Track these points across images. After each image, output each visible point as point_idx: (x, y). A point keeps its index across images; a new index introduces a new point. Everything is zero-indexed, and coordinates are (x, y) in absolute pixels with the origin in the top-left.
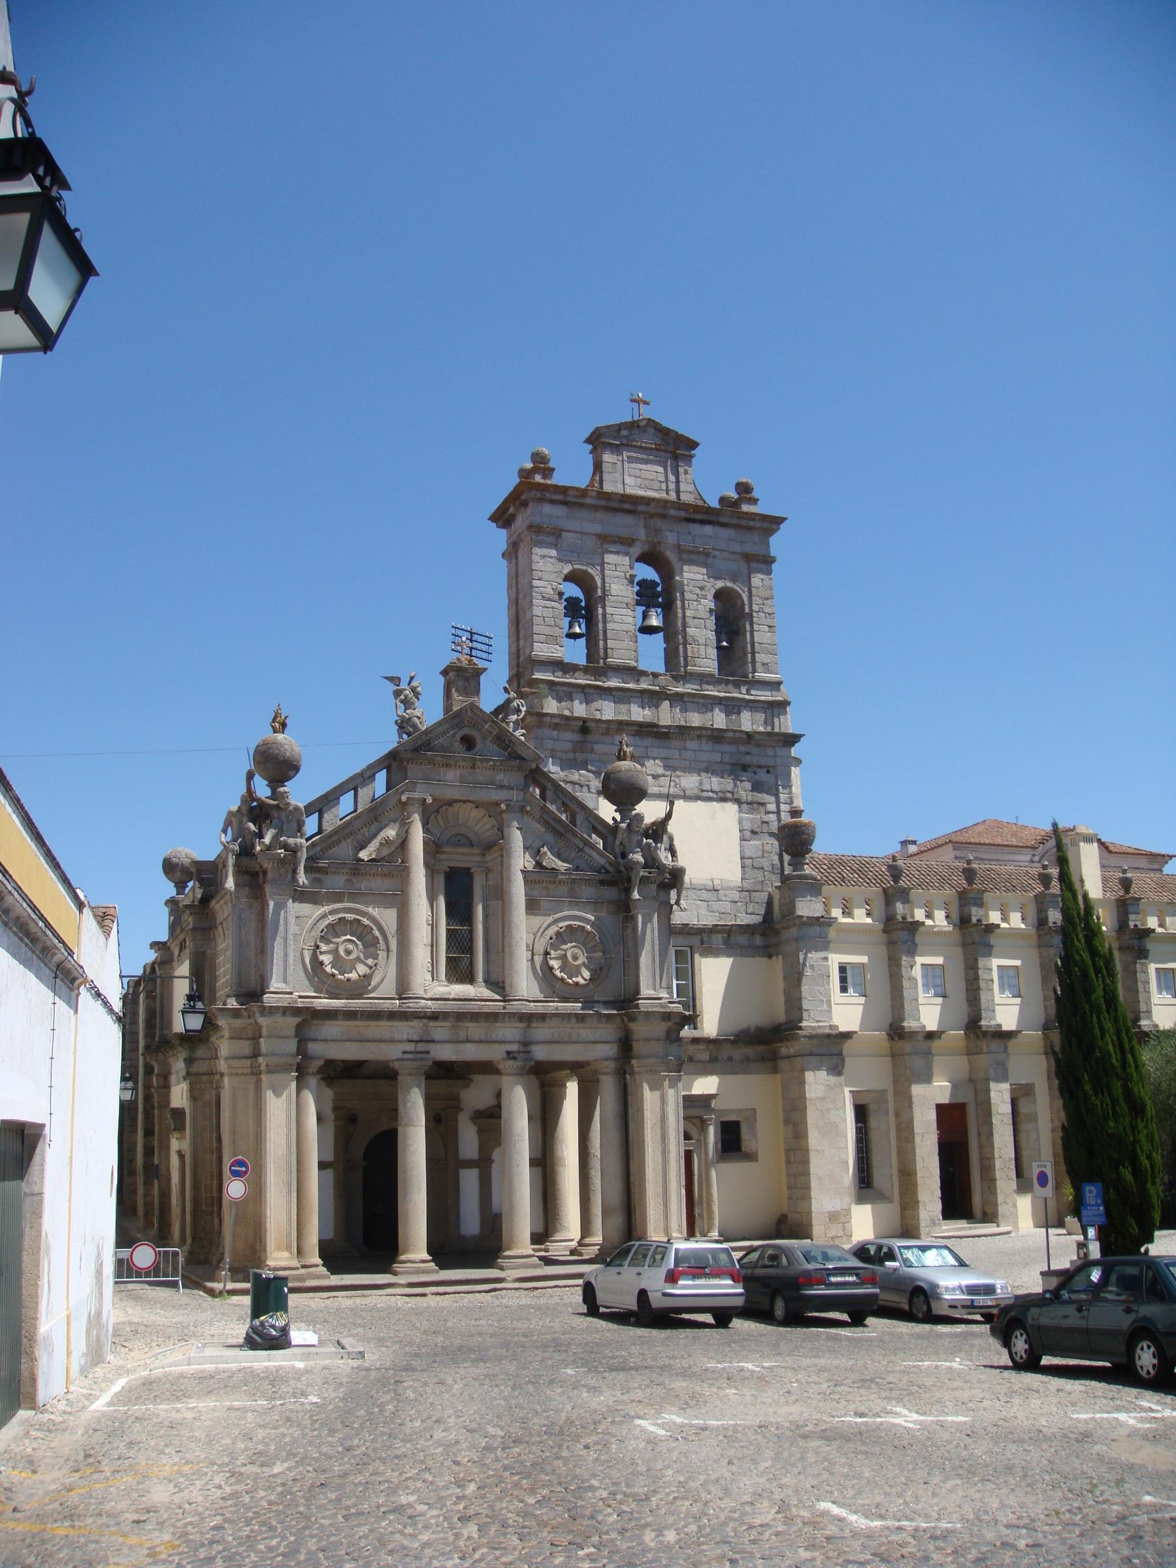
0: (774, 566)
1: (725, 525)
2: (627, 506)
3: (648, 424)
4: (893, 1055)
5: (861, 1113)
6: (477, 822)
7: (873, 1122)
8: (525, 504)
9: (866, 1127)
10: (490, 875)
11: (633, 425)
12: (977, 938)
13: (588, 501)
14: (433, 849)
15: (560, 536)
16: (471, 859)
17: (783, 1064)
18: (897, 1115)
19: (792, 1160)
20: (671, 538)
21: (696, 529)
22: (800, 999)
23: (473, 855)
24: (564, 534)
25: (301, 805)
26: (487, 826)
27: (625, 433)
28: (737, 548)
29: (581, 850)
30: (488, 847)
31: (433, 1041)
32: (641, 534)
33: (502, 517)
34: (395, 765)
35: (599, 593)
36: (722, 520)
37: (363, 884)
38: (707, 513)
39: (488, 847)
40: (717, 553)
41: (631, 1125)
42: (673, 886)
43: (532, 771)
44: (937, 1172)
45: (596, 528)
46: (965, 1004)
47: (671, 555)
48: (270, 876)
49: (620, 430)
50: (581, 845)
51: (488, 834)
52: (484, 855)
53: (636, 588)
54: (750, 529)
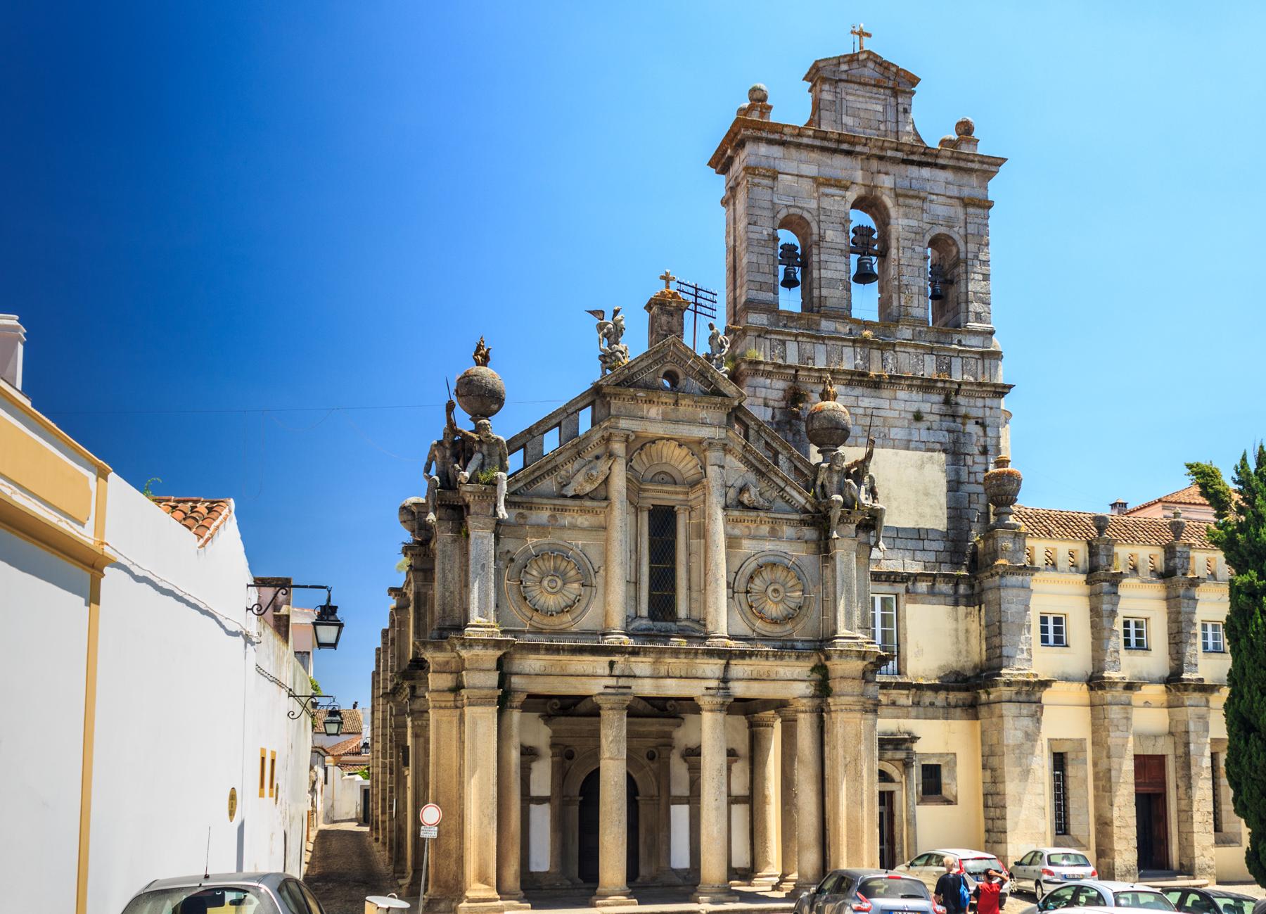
4: (1092, 705)
5: (1059, 761)
6: (680, 461)
7: (1071, 771)
8: (741, 145)
9: (1064, 775)
10: (693, 514)
12: (1182, 591)
14: (635, 486)
15: (774, 178)
16: (674, 497)
17: (983, 711)
18: (1095, 764)
19: (990, 803)
20: (886, 182)
22: (1001, 647)
23: (676, 493)
25: (503, 439)
26: (691, 465)
28: (954, 191)
29: (783, 489)
30: (694, 484)
31: (635, 677)
32: (859, 176)
33: (721, 163)
34: (598, 402)
35: (815, 238)
37: (567, 519)
39: (694, 484)
40: (934, 197)
41: (827, 762)
42: (873, 527)
43: (734, 409)
44: (1133, 822)
46: (1168, 657)
48: (472, 510)
50: (782, 485)
51: (692, 472)
52: (687, 493)
53: (852, 235)
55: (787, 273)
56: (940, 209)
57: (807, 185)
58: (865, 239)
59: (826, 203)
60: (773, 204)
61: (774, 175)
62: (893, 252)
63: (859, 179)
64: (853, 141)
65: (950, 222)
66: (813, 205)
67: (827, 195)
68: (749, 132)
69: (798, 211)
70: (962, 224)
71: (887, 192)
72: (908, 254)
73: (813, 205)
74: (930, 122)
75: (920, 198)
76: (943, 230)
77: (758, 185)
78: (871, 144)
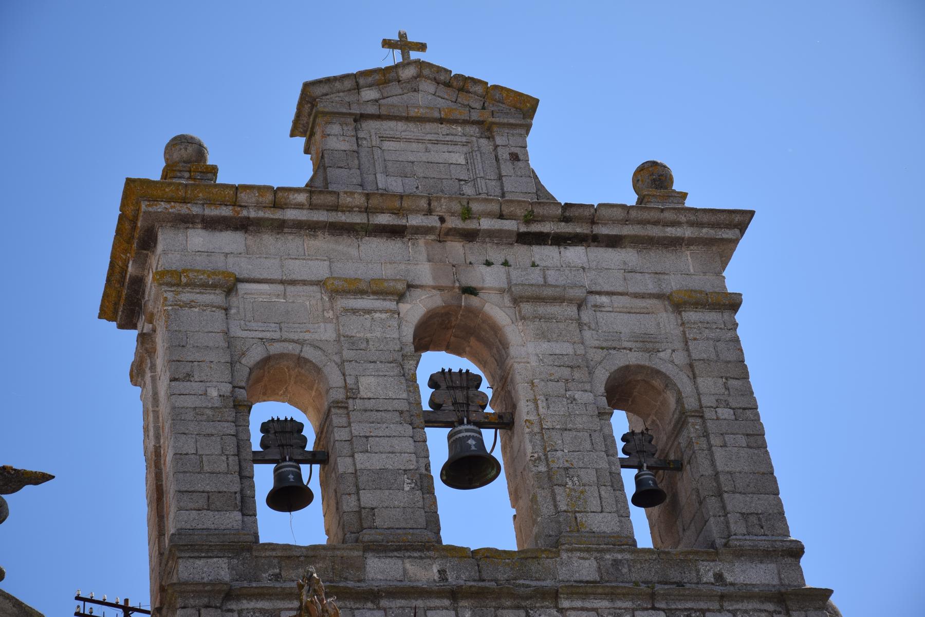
0: (739, 317)
1: (614, 242)
2: (384, 219)
3: (419, 76)
11: (383, 77)
13: (291, 214)
15: (230, 290)
20: (490, 278)
21: (547, 254)
24: (242, 287)
27: (369, 94)
32: (424, 273)
36: (603, 230)
38: (566, 220)
40: (604, 299)
45: (320, 270)
47: (498, 312)
49: (358, 88)
54: (674, 243)
55: (279, 477)
56: (618, 321)
57: (309, 300)
58: (460, 396)
59: (355, 327)
60: (230, 341)
61: (230, 285)
62: (524, 411)
63: (424, 273)
64: (399, 203)
65: (648, 343)
66: (326, 333)
67: (354, 311)
68: (161, 207)
69: (290, 348)
70: (678, 345)
71: (495, 297)
72: (560, 408)
73: (326, 333)
74: (578, 164)
75: (570, 301)
76: (633, 358)
77: (190, 305)
78: (441, 207)
